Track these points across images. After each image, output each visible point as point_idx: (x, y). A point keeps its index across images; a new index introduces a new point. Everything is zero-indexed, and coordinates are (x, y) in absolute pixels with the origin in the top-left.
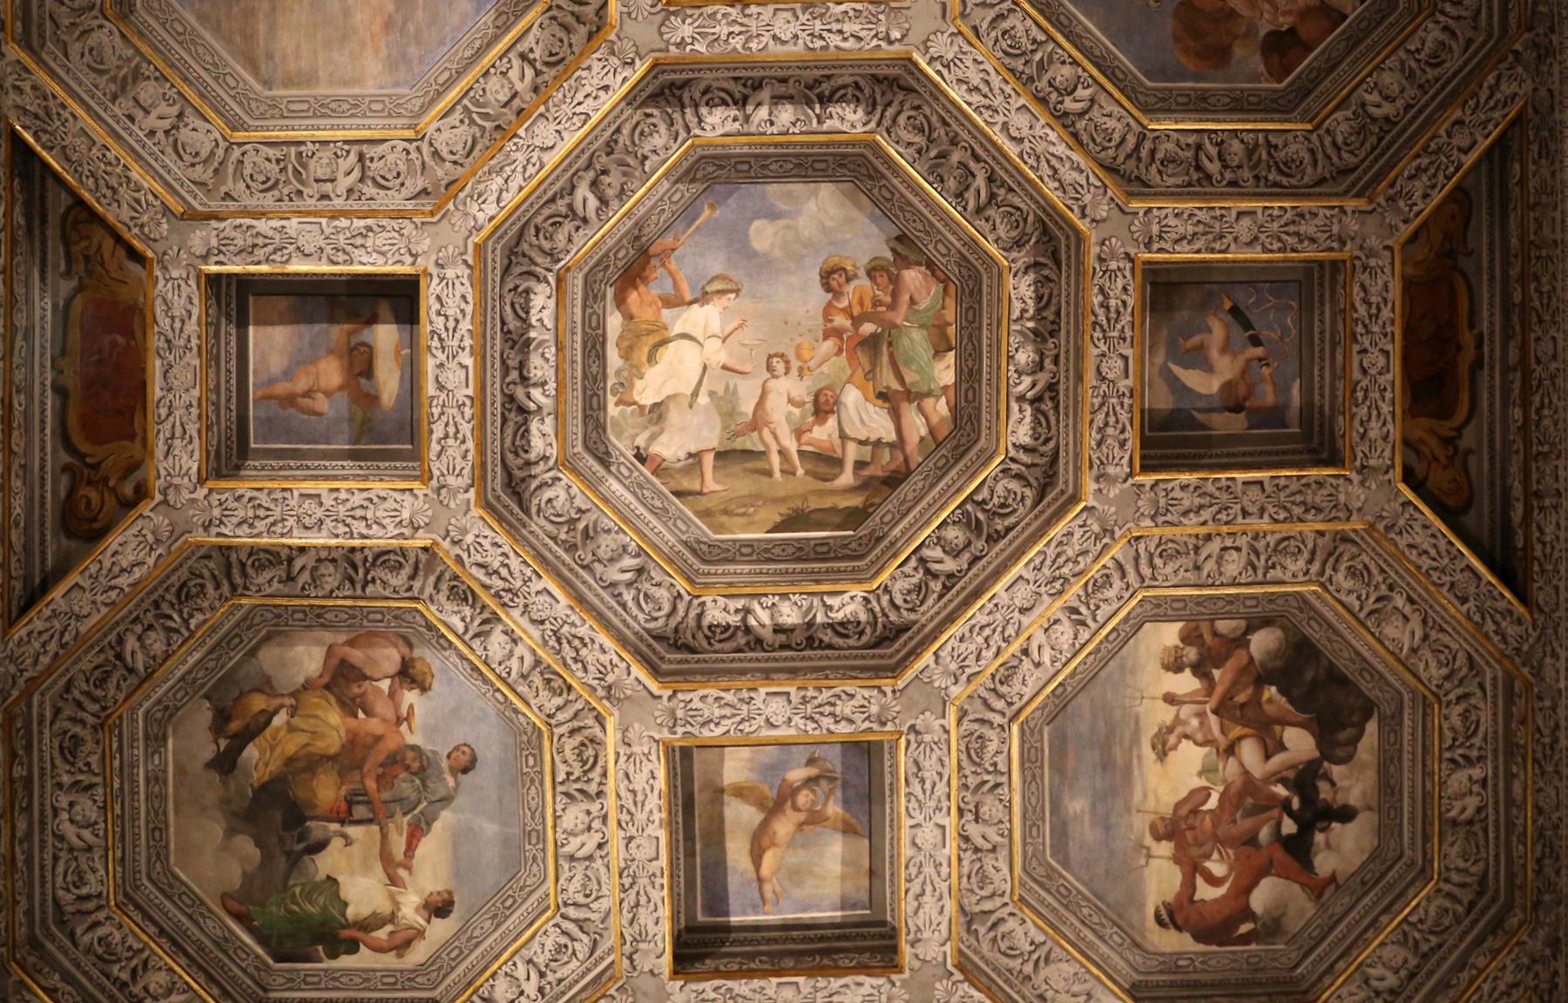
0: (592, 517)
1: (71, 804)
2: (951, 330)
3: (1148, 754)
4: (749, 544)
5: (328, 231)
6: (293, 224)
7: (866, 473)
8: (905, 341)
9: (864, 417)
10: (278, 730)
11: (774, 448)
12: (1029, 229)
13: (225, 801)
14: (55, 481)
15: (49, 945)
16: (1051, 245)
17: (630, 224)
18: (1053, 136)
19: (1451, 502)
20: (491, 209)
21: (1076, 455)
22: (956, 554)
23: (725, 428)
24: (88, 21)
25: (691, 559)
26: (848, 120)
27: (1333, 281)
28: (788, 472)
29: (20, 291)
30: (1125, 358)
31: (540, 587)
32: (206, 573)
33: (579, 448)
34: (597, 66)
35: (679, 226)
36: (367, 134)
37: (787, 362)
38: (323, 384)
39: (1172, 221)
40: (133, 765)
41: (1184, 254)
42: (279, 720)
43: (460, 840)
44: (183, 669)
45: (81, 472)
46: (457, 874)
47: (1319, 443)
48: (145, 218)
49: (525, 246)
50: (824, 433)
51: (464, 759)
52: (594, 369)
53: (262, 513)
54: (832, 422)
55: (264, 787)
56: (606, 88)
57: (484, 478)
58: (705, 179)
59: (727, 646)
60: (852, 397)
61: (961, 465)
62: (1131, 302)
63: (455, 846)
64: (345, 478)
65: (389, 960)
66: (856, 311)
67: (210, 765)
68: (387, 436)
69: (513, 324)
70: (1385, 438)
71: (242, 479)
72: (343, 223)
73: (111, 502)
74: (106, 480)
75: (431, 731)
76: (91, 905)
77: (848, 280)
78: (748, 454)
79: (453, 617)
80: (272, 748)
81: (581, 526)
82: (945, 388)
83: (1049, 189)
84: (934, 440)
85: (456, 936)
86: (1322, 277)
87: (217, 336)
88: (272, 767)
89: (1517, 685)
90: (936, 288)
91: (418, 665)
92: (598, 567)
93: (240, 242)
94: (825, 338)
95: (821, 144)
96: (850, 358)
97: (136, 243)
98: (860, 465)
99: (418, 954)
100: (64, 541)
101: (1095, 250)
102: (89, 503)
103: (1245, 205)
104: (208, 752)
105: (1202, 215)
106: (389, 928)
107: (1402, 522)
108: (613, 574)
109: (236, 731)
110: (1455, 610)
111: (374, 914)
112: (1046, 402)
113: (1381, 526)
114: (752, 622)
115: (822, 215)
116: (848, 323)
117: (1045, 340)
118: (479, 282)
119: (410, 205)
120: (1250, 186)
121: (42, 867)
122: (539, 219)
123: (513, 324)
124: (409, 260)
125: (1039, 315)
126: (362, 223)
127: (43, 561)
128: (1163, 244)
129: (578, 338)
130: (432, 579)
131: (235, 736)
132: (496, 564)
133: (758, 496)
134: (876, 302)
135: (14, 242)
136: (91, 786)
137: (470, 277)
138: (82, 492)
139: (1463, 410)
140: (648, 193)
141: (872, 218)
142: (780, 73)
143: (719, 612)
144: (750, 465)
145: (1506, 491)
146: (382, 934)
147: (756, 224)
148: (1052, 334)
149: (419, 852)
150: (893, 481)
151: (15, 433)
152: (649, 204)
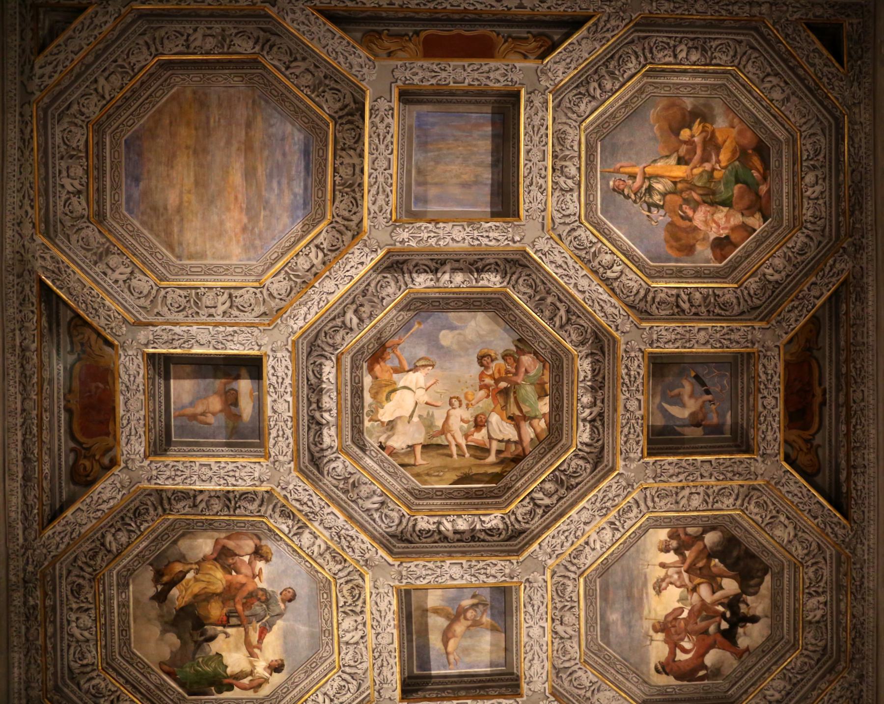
0: (357, 476)
1: (77, 619)
2: (547, 386)
5: (213, 333)
6: (194, 329)
7: (502, 456)
8: (523, 391)
9: (501, 428)
10: (189, 581)
11: (453, 443)
12: (588, 336)
13: (161, 616)
14: (67, 456)
15: (66, 690)
16: (600, 344)
17: (375, 331)
18: (601, 290)
19: (809, 470)
21: (614, 448)
23: (427, 433)
24: (81, 224)
26: (492, 281)
27: (748, 363)
28: (461, 455)
29: (45, 360)
30: (639, 401)
31: (329, 510)
32: (149, 503)
33: (349, 443)
34: (357, 252)
35: (401, 333)
36: (233, 284)
37: (460, 401)
38: (211, 409)
39: (664, 333)
40: (111, 599)
41: (670, 349)
42: (190, 576)
43: (286, 635)
44: (137, 550)
45: (80, 451)
46: (286, 651)
47: (740, 441)
48: (113, 325)
49: (319, 342)
50: (480, 436)
52: (357, 403)
53: (179, 473)
54: (484, 431)
55: (182, 609)
56: (362, 263)
57: (299, 456)
58: (415, 310)
59: (429, 540)
60: (494, 418)
61: (552, 452)
62: (642, 372)
63: (285, 637)
64: (224, 456)
65: (250, 694)
66: (497, 376)
67: (153, 598)
68: (247, 436)
69: (313, 380)
70: (775, 440)
71: (168, 456)
72: (221, 329)
73: (97, 467)
74: (94, 456)
75: (271, 582)
76: (89, 669)
77: (492, 361)
78: (439, 446)
79: (283, 526)
80: (186, 590)
81: (351, 481)
82: (544, 415)
83: (599, 317)
84: (538, 440)
85: (286, 682)
86: (742, 361)
87: (153, 384)
88: (186, 599)
89: (843, 558)
90: (539, 365)
91: (264, 549)
94: (481, 389)
95: (478, 293)
96: (494, 399)
97: (109, 337)
98: (499, 452)
99: (265, 691)
100: (72, 486)
101: (623, 347)
102: (85, 468)
103: (702, 325)
104: (152, 591)
105: (679, 330)
106: (250, 678)
107: (783, 480)
108: (368, 505)
109: (166, 581)
110: (811, 522)
111: (242, 671)
112: (598, 422)
113: (773, 483)
115: (478, 326)
116: (492, 382)
117: (597, 391)
118: (295, 359)
119: (257, 320)
120: (705, 315)
121: (62, 650)
122: (327, 328)
123: (313, 380)
124: (257, 348)
125: (593, 379)
127: (61, 495)
129: (349, 388)
130: (271, 507)
131: (165, 584)
132: (305, 500)
134: (507, 372)
135: (42, 336)
136: (88, 609)
137: (290, 357)
138: (82, 462)
139: (816, 426)
140: (385, 316)
141: (505, 330)
142: (458, 257)
143: (424, 523)
144: (441, 451)
145: (838, 465)
146: (246, 681)
147: (443, 332)
148: (600, 388)
149: (266, 641)
150: (517, 460)
151: (44, 432)
152: (385, 321)
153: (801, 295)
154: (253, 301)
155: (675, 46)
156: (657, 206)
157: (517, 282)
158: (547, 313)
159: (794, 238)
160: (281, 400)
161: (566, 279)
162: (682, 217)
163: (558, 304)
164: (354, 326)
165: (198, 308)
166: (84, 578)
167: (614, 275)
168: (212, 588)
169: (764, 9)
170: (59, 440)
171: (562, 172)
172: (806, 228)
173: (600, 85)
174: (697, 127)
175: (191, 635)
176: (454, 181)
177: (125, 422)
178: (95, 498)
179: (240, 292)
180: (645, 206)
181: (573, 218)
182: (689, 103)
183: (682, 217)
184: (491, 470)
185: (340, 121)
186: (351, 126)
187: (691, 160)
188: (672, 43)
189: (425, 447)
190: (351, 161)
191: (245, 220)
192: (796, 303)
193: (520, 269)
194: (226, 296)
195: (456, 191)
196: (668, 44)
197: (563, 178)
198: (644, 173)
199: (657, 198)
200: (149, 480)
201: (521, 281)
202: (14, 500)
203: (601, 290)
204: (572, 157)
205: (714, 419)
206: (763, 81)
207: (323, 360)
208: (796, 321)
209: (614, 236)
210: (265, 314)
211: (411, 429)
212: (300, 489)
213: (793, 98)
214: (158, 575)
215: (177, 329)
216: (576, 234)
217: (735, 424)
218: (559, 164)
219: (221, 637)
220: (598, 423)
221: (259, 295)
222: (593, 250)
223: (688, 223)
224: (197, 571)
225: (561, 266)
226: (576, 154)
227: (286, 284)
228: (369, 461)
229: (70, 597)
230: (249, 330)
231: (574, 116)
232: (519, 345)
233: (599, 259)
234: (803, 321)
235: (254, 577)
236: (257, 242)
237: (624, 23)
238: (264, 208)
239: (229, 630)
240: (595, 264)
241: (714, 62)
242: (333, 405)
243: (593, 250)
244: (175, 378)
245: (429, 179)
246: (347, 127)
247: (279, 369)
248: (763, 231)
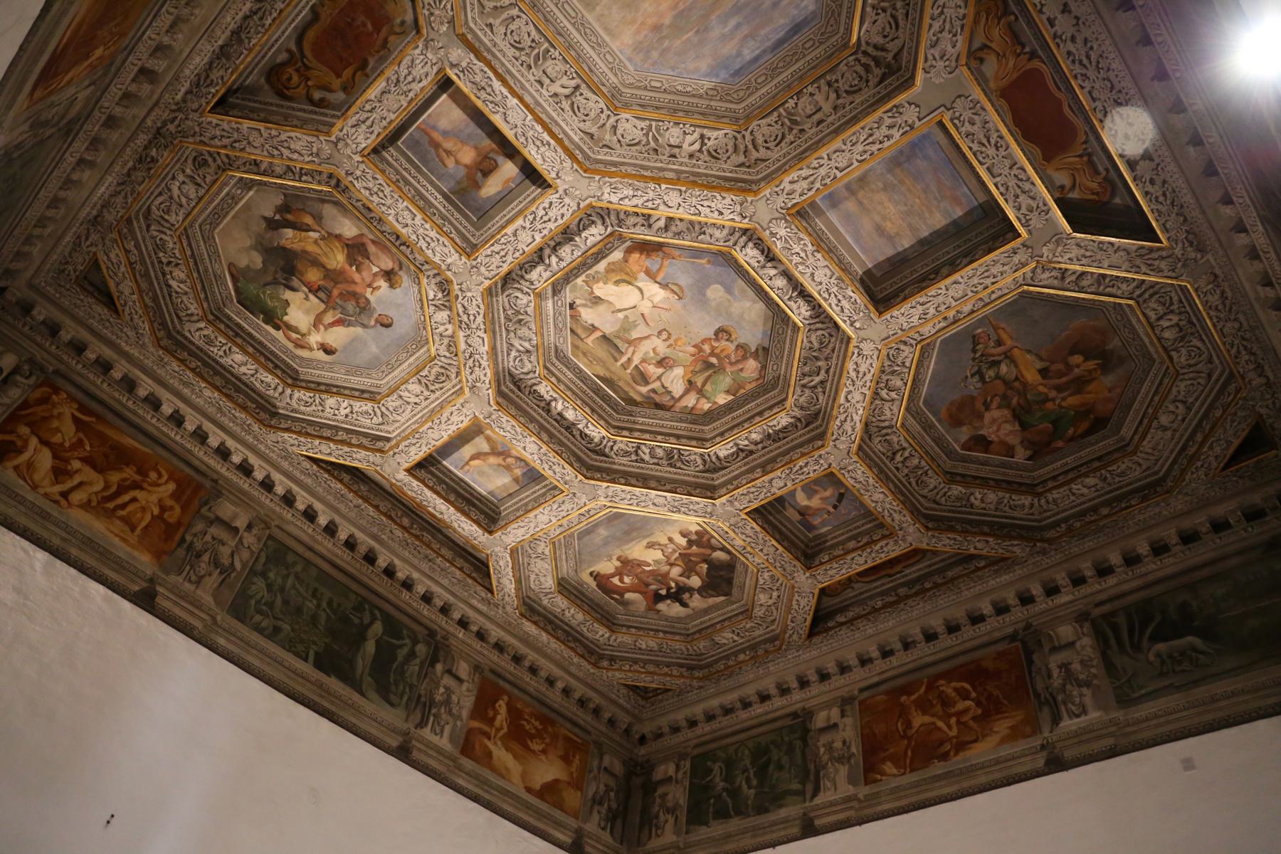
0: (528, 319)
3: (645, 543)
4: (581, 371)
5: (527, 122)
14: (279, 50)
20: (614, 198)
22: (652, 456)
25: (553, 353)
38: (460, 156)
48: (437, 12)
51: (385, 321)
55: (284, 249)
67: (265, 218)
72: (539, 128)
73: (302, 90)
74: (308, 79)
92: (512, 335)
93: (478, 79)
100: (263, 80)
102: (290, 79)
114: (553, 404)
124: (553, 175)
126: (548, 138)
131: (286, 220)
133: (604, 363)
137: (574, 212)
154: (592, 114)
160: (529, 233)
164: (656, 226)
165: (536, 63)
166: (215, 160)
168: (324, 260)
170: (283, 33)
174: (1091, 364)
175: (276, 272)
176: (877, 218)
177: (368, 107)
178: (283, 137)
179: (590, 95)
180: (976, 369)
182: (1114, 343)
184: (632, 394)
185: (860, 56)
186: (863, 73)
189: (604, 337)
190: (822, 103)
191: (667, 21)
194: (573, 83)
195: (867, 225)
200: (347, 174)
202: (198, 60)
205: (816, 521)
207: (599, 222)
209: (926, 363)
210: (592, 136)
211: (610, 317)
212: (474, 302)
214: (284, 208)
215: (497, 84)
217: (824, 535)
219: (300, 295)
220: (742, 455)
221: (603, 116)
223: (983, 408)
224: (323, 238)
227: (638, 135)
228: (550, 304)
229: (190, 161)
230: (563, 156)
232: (760, 351)
235: (369, 286)
236: (655, 55)
238: (697, 32)
239: (311, 297)
242: (568, 259)
244: (450, 96)
245: (861, 194)
246: (859, 68)
247: (555, 210)
248: (1016, 463)
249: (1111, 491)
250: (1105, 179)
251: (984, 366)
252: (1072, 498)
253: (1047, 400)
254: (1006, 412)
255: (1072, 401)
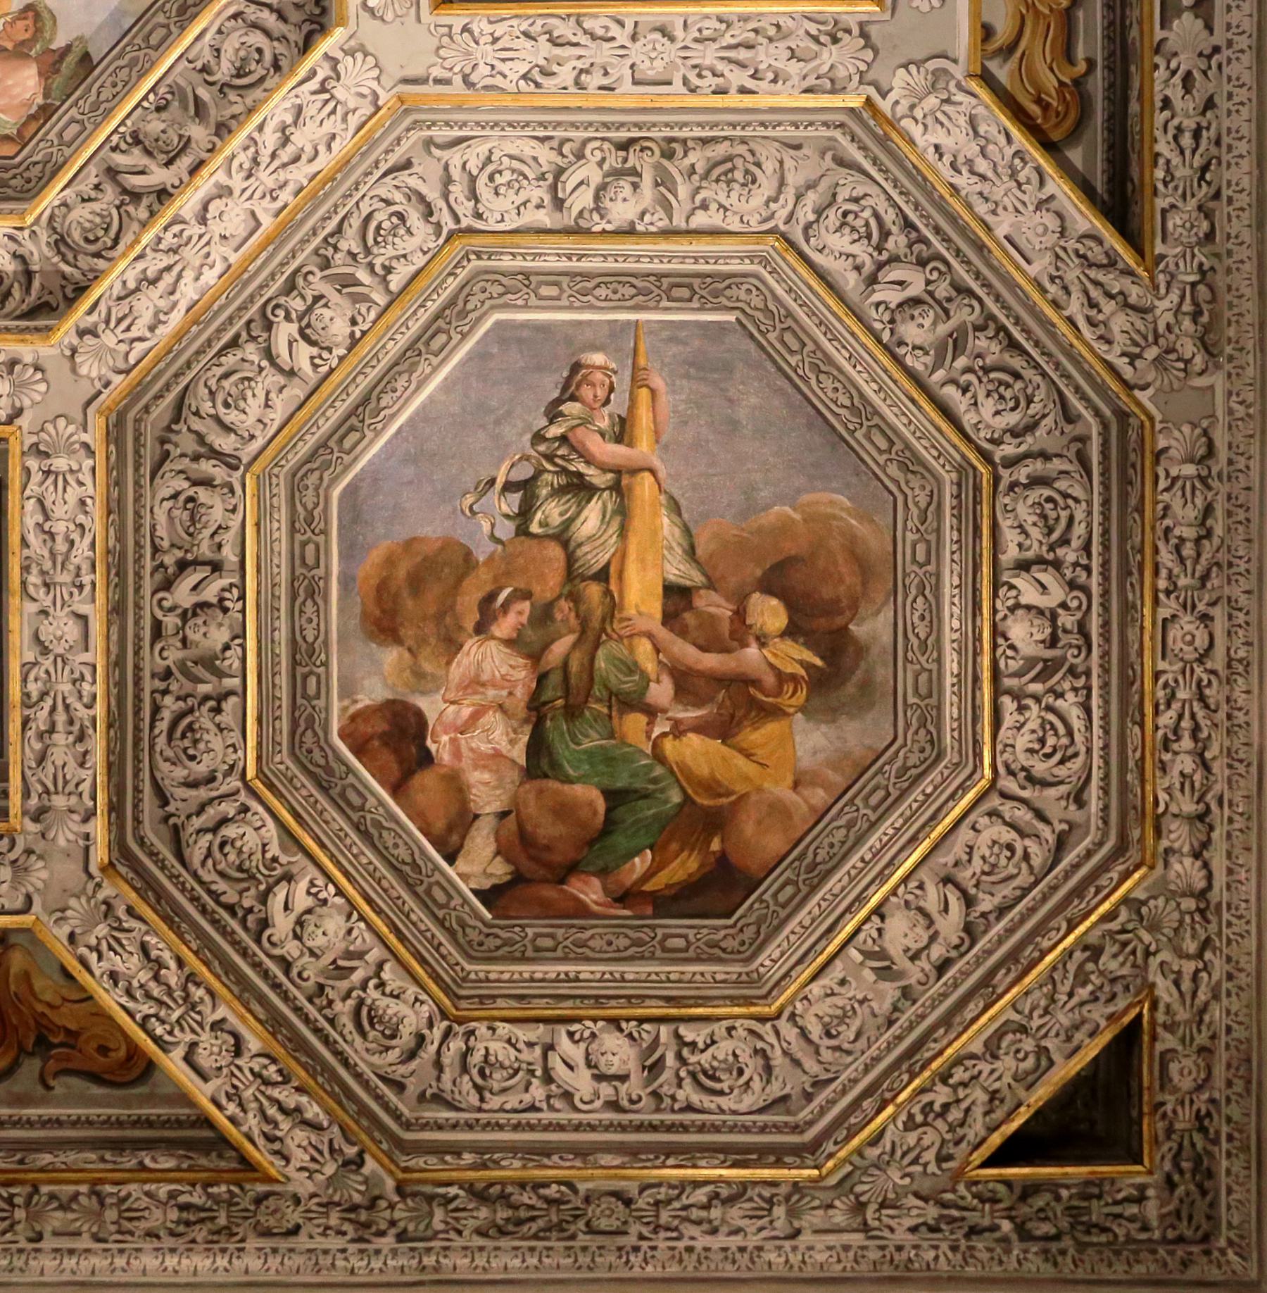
128: (37, 477)
153: (198, 993)
155: (1057, 565)
156: (525, 514)
157: (254, 26)
158: (155, 126)
159: (412, 990)
161: (244, 158)
162: (491, 597)
163: (185, 162)
167: (281, 348)
169: (1185, 869)
171: (618, 173)
172: (447, 1034)
173: (916, 302)
174: (795, 656)
180: (524, 472)
181: (465, 208)
182: (873, 627)
183: (491, 597)
187: (683, 633)
188: (1069, 555)
192: (172, 976)
193: (296, 36)
196: (1065, 541)
197: (596, 177)
198: (634, 472)
199: (551, 512)
201: (257, 39)
203: (210, 276)
204: (668, 208)
206: (947, 880)
208: (114, 976)
213: (890, 991)
216: (414, 219)
218: (645, 163)
222: (362, 275)
225: (286, 141)
226: (679, 222)
231: (806, 213)
232: (71, 59)
233: (334, 297)
234: (111, 999)
237: (1121, 363)
240: (318, 284)
241: (1008, 704)
243: (362, 275)
248: (450, 889)
249: (653, 1128)
250: (1077, 82)
251: (550, 478)
252: (538, 1092)
253: (633, 702)
254: (520, 674)
255: (696, 752)
